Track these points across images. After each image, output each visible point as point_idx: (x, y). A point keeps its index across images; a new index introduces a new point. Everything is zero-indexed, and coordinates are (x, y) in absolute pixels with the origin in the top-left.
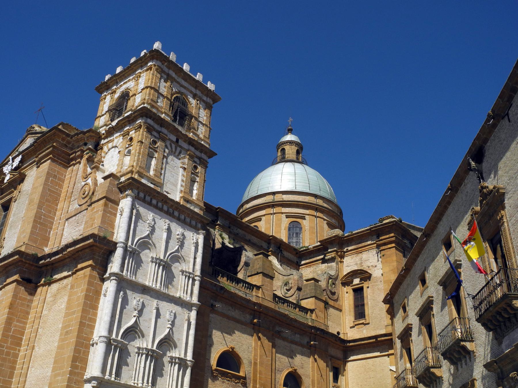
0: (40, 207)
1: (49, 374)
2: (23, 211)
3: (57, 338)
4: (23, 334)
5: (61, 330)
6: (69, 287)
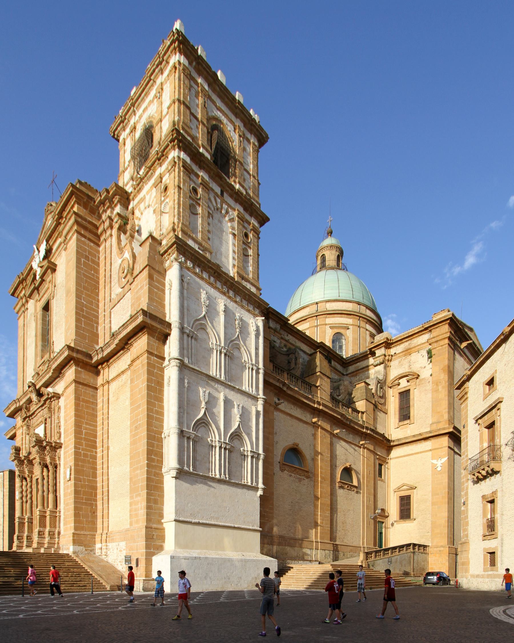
0: (78, 296)
1: (128, 469)
2: (63, 307)
3: (128, 435)
4: (95, 436)
5: (130, 427)
6: (129, 381)
